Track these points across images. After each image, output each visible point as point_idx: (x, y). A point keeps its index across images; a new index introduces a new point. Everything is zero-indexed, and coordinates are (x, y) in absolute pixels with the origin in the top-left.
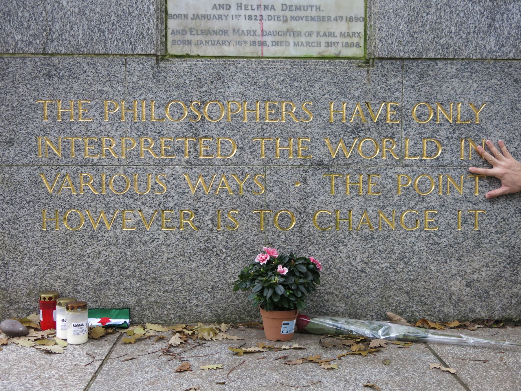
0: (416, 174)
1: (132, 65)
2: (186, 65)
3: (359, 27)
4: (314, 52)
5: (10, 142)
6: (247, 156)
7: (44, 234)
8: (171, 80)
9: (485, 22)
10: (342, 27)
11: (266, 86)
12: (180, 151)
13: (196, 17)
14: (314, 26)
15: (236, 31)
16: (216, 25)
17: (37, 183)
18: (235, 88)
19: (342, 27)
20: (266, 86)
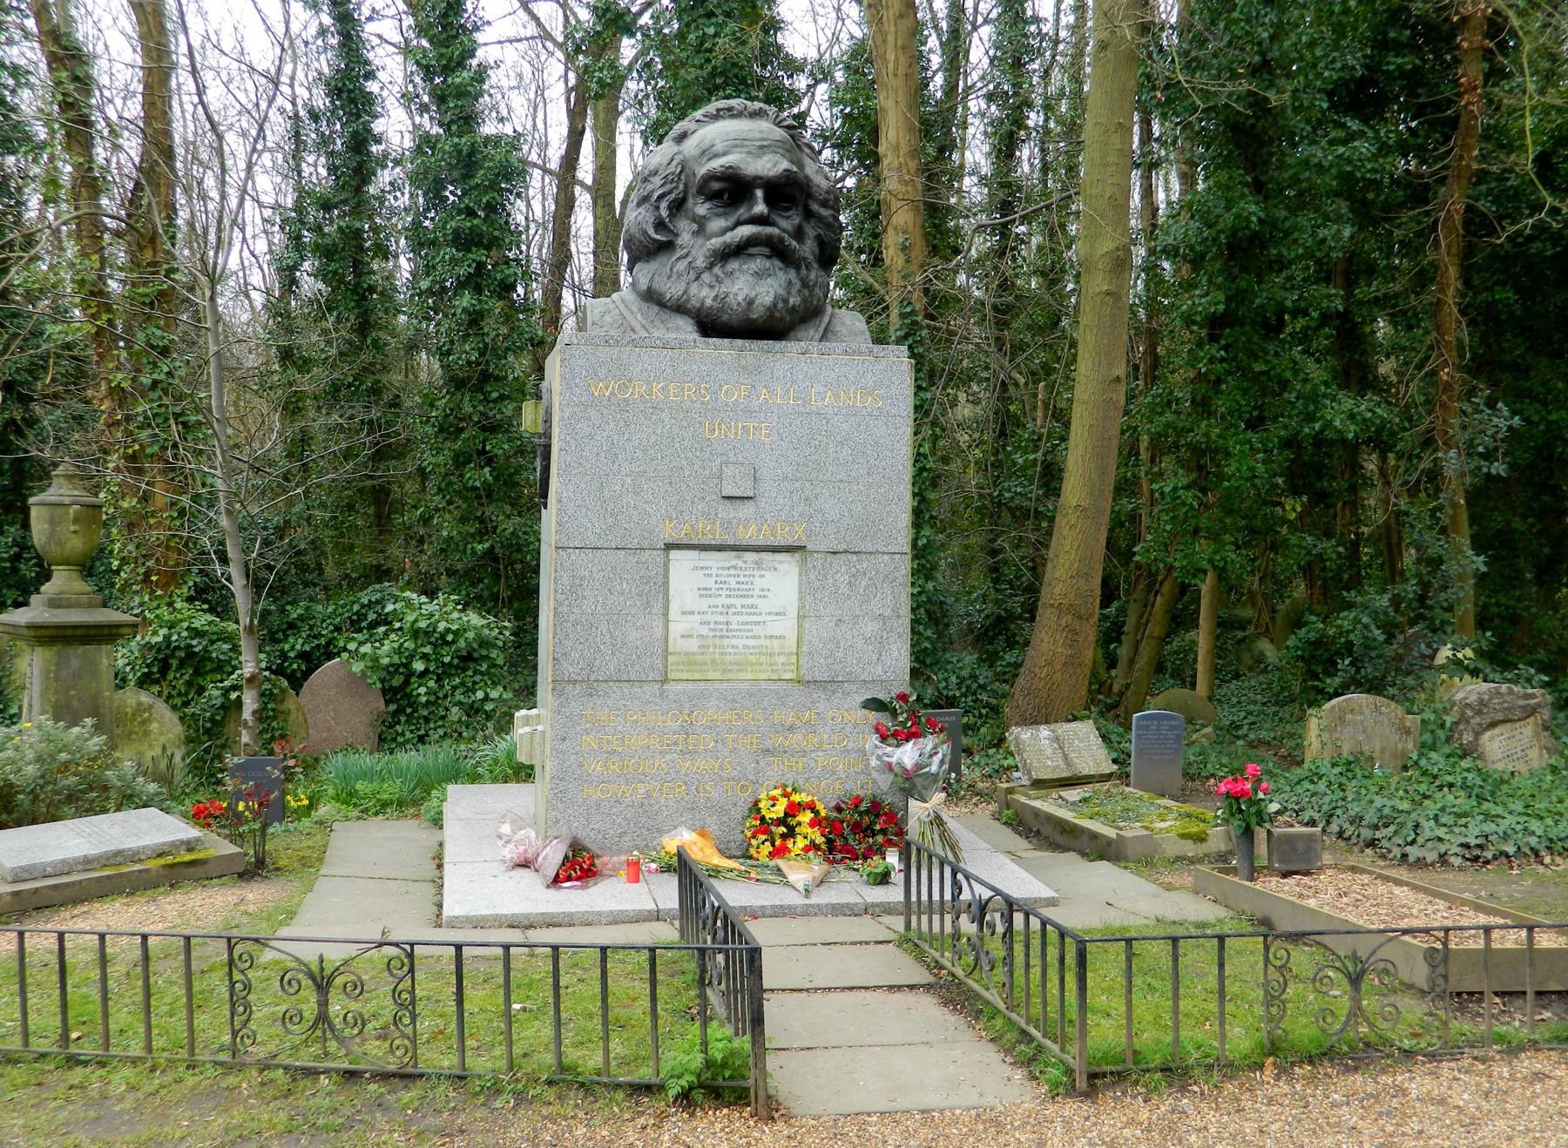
0: (831, 756)
1: (646, 687)
2: (680, 686)
3: (793, 659)
4: (763, 676)
5: (564, 739)
6: (720, 746)
7: (584, 800)
8: (672, 696)
9: (875, 657)
10: (782, 659)
11: (734, 701)
12: (676, 743)
13: (687, 654)
14: (763, 659)
15: (713, 661)
16: (699, 658)
17: (580, 765)
18: (714, 702)
19: (782, 659)
20: (734, 701)
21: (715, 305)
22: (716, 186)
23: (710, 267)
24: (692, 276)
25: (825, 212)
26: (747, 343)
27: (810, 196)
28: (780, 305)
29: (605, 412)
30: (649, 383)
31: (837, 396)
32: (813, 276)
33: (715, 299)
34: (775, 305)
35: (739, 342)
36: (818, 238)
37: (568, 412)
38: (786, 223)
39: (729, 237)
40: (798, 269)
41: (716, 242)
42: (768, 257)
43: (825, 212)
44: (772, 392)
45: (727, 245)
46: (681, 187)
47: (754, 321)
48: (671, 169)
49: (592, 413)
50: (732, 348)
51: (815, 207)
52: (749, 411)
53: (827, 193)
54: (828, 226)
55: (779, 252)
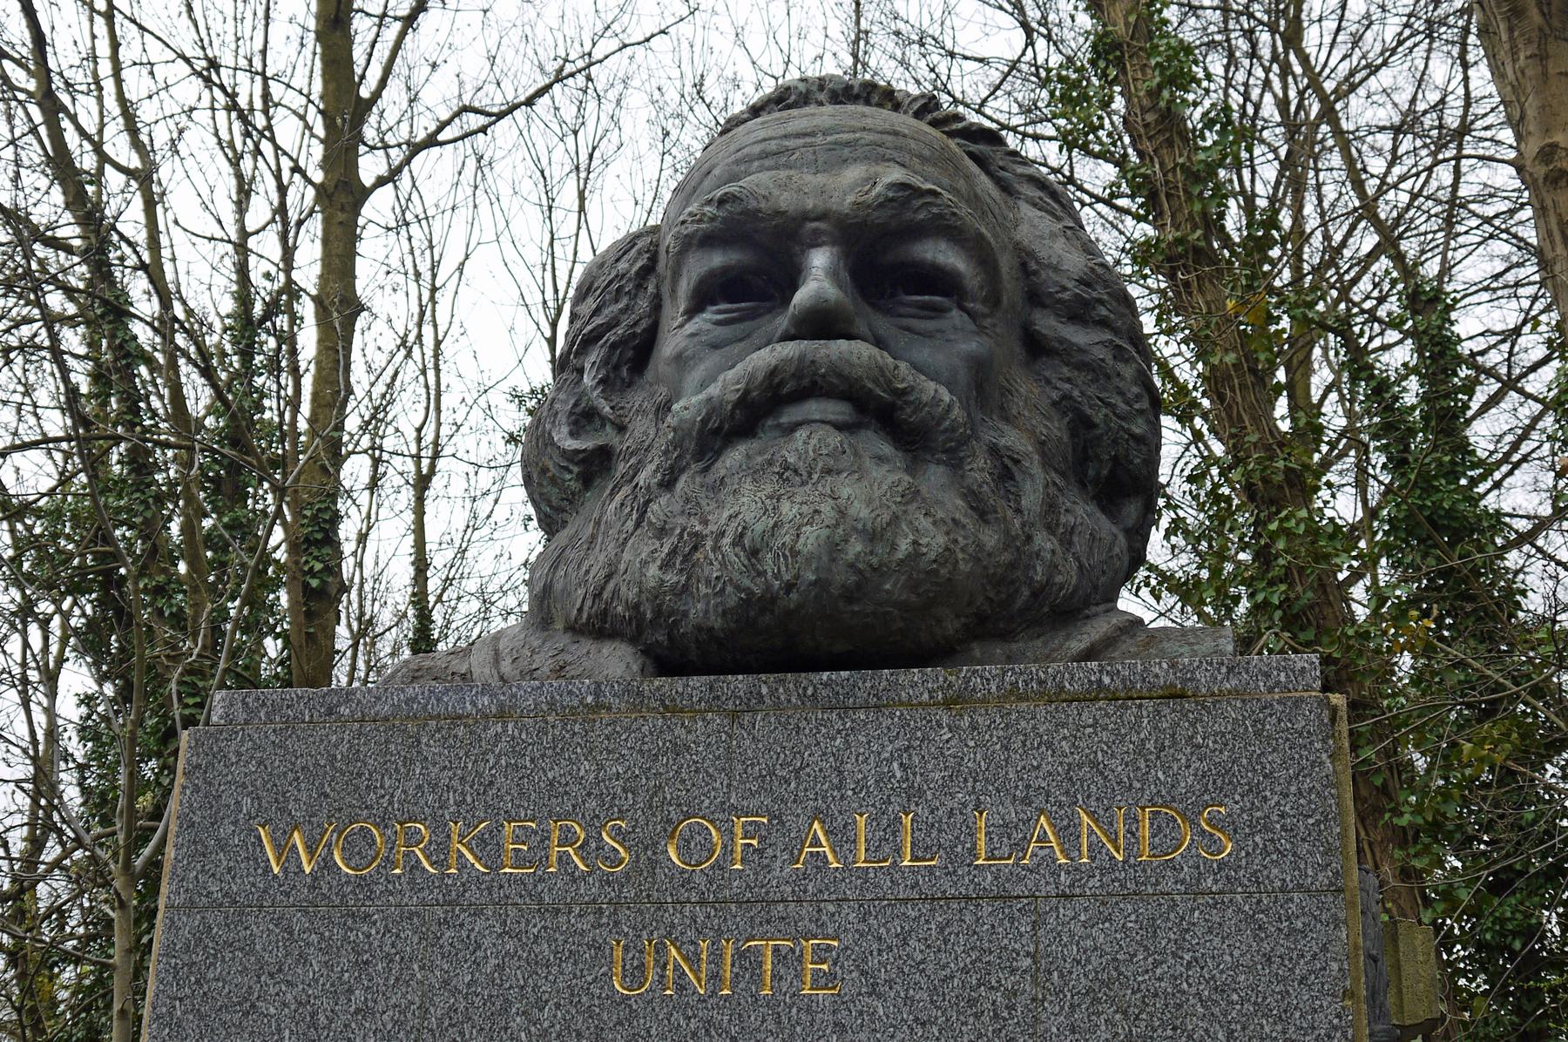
21: (671, 578)
22: (699, 265)
23: (668, 484)
24: (630, 525)
25: (1079, 336)
26: (765, 684)
27: (1035, 298)
28: (856, 547)
29: (299, 921)
30: (439, 826)
31: (1069, 834)
32: (1032, 497)
33: (666, 565)
34: (834, 548)
35: (740, 683)
36: (1064, 405)
37: (189, 924)
38: (928, 363)
39: (714, 390)
40: (955, 464)
41: (689, 405)
42: (839, 427)
43: (1079, 336)
44: (841, 836)
45: (713, 407)
46: (643, 304)
47: (767, 601)
48: (622, 266)
49: (259, 927)
50: (714, 703)
51: (1048, 324)
52: (760, 906)
53: (1083, 282)
54: (1095, 371)
55: (880, 412)
